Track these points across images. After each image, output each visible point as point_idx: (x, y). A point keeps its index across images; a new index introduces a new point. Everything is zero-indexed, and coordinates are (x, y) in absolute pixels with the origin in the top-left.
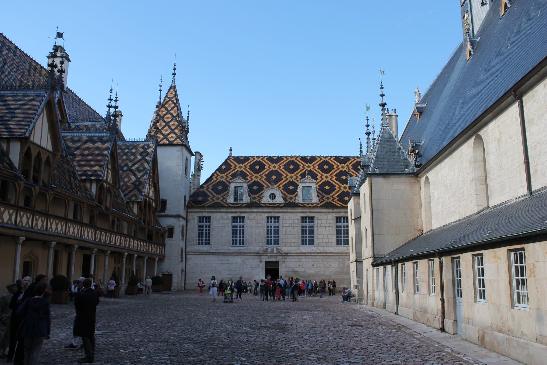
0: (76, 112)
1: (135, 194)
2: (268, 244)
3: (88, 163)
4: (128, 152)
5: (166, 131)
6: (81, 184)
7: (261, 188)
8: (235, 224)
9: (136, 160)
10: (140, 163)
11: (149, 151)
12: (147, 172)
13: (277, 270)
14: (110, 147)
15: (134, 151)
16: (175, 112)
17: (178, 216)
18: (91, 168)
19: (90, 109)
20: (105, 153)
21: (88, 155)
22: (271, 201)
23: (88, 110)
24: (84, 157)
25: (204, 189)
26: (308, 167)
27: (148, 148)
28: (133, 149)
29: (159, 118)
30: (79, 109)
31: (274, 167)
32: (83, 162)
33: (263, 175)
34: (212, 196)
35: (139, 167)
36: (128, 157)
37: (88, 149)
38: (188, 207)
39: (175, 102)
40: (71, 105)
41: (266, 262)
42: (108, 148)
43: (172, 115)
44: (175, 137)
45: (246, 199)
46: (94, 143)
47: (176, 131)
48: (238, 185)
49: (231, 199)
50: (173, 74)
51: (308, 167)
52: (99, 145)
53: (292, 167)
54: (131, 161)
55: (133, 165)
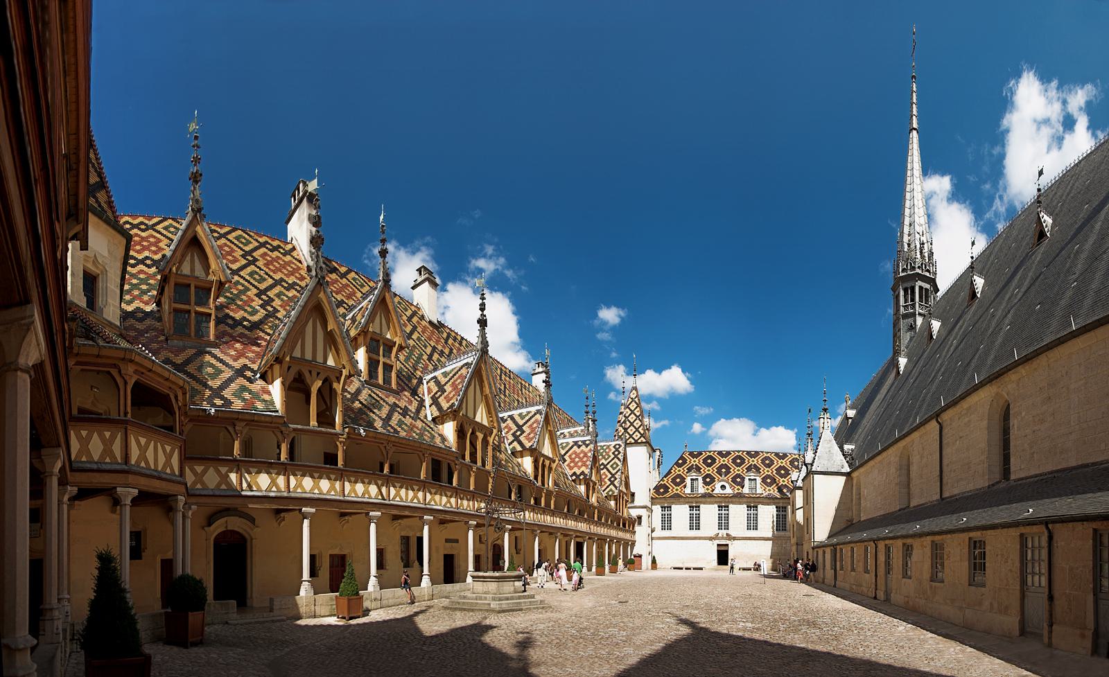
2: (719, 529)
3: (576, 465)
5: (631, 430)
7: (713, 480)
8: (692, 512)
9: (610, 459)
11: (620, 450)
13: (727, 552)
15: (607, 450)
17: (645, 507)
22: (722, 492)
24: (572, 461)
25: (665, 482)
26: (754, 461)
27: (619, 448)
31: (724, 461)
32: (572, 465)
33: (714, 469)
34: (671, 488)
35: (613, 465)
37: (575, 452)
38: (652, 498)
41: (718, 545)
44: (639, 435)
45: (702, 489)
46: (579, 447)
47: (640, 430)
48: (694, 477)
49: (688, 490)
51: (754, 461)
52: (583, 448)
53: (738, 461)
54: (606, 460)
55: (608, 463)
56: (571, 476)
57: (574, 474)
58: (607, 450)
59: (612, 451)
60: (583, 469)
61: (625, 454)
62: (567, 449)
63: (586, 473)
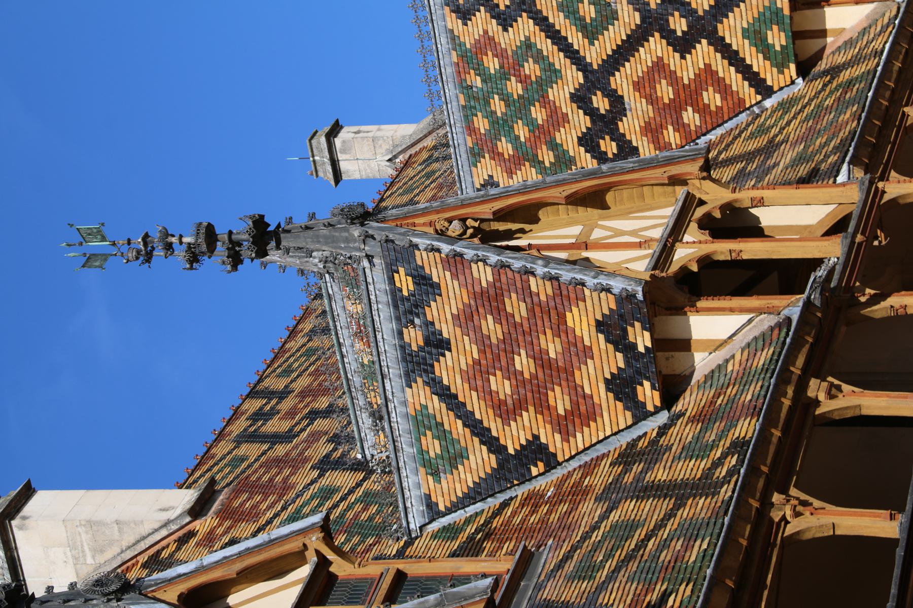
0: (314, 415)
1: (746, 33)
4: (506, 99)
6: (689, 402)
9: (545, 45)
14: (446, 248)
15: (492, 64)
18: (587, 352)
19: (307, 326)
20: (484, 275)
21: (511, 373)
23: (313, 332)
24: (531, 395)
28: (481, 71)
30: (303, 394)
32: (560, 401)
36: (538, 92)
37: (478, 374)
40: (281, 450)
42: (455, 262)
46: (438, 344)
52: (442, 313)
54: (552, 75)
56: (640, 413)
57: (621, 387)
58: (492, 64)
59: (494, 27)
60: (581, 321)
62: (458, 428)
63: (608, 303)
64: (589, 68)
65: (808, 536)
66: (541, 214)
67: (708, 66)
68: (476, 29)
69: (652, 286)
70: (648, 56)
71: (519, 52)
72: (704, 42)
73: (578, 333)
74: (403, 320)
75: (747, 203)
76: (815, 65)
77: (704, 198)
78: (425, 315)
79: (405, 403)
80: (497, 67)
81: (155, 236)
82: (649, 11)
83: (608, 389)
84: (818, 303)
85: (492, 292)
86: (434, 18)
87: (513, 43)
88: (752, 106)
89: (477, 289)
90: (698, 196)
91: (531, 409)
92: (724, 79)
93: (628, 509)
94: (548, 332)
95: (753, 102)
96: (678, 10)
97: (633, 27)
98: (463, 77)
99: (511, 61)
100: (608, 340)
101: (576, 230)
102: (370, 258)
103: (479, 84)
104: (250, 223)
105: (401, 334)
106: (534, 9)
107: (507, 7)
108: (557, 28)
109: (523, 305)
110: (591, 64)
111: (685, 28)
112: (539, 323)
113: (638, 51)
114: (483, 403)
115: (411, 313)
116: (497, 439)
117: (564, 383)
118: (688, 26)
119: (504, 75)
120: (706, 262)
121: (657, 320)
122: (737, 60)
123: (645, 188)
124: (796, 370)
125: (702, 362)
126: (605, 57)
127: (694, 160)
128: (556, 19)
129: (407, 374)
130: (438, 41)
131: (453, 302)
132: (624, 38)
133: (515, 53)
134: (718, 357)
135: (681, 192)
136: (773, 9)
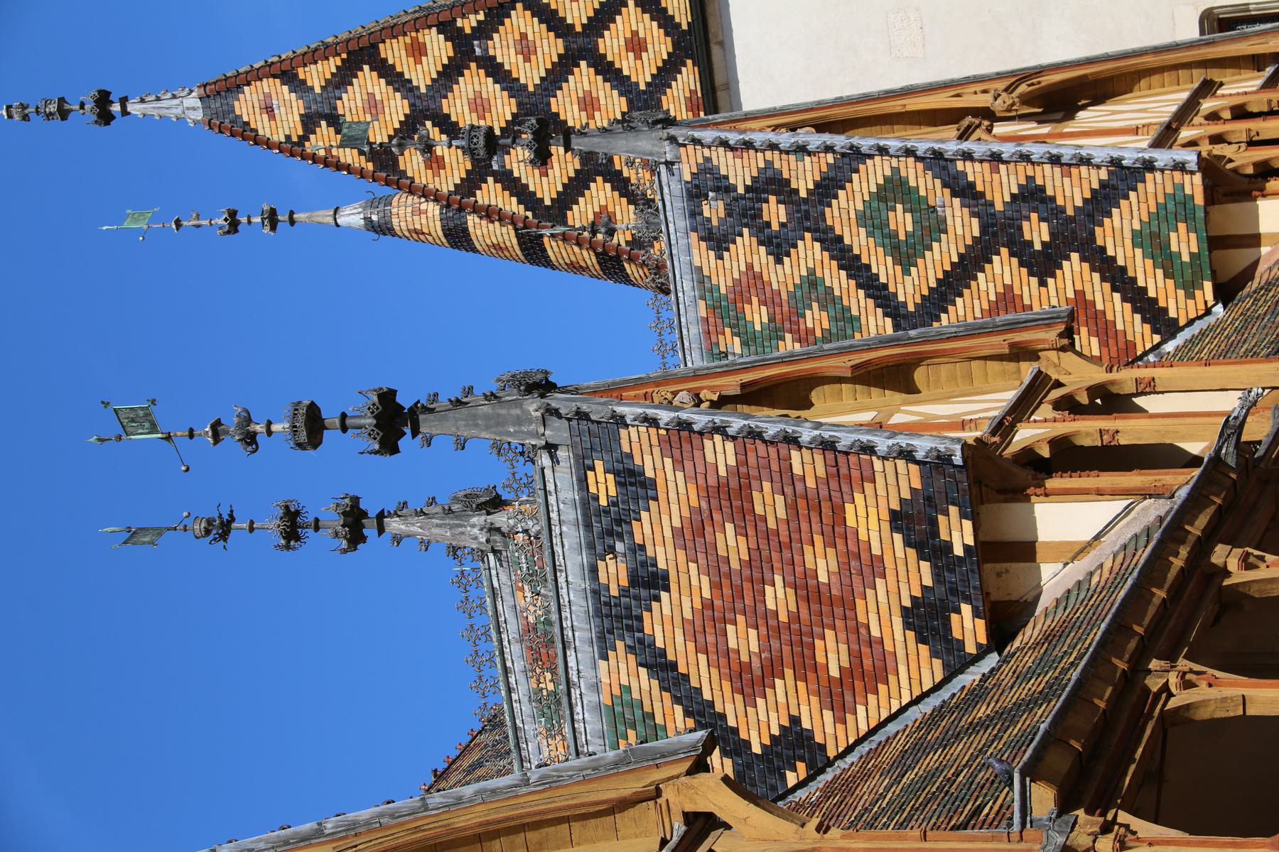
6: (1030, 633)
9: (837, 280)
10: (859, 241)
11: (739, 172)
12: (936, 161)
14: (665, 416)
15: (757, 316)
16: (417, 51)
18: (876, 567)
21: (760, 618)
24: (790, 651)
29: (491, 193)
32: (833, 654)
37: (707, 625)
39: (332, 64)
43: (450, 74)
46: (650, 581)
50: (105, 117)
52: (656, 530)
57: (927, 619)
58: (757, 316)
61: (790, 118)
63: (911, 478)
64: (902, 311)
65: (1203, 714)
66: (815, 396)
67: (1080, 294)
68: (735, 264)
69: (977, 452)
70: (991, 285)
71: (799, 294)
72: (1075, 256)
73: (863, 536)
74: (599, 548)
75: (1130, 388)
76: (1243, 288)
77: (1063, 379)
78: (632, 534)
79: (596, 687)
80: (765, 320)
81: (231, 422)
82: (993, 215)
83: (907, 626)
84: (1231, 461)
85: (734, 484)
86: (674, 252)
87: (790, 281)
88: (1146, 353)
89: (712, 481)
90: (1054, 377)
91: (789, 673)
92: (1104, 312)
93: (932, 760)
94: (818, 539)
95: (1148, 346)
96: (1035, 210)
97: (969, 242)
98: (714, 339)
99: (786, 308)
100: (908, 543)
101: (867, 417)
102: (551, 448)
103: (738, 350)
104: (375, 399)
105: (594, 570)
106: (822, 226)
107: (782, 225)
108: (856, 251)
109: (780, 499)
110: (905, 304)
111: (1046, 238)
112: (805, 526)
113: (976, 279)
114: (714, 671)
115: (610, 533)
116: (735, 731)
117: (839, 623)
118: (1051, 234)
119: (775, 332)
120: (1061, 445)
121: (983, 509)
122: (1124, 282)
123: (975, 364)
124: (1197, 528)
125: (1053, 578)
126: (926, 292)
127: (1048, 325)
128: (855, 239)
129: (602, 638)
130: (679, 288)
131: (674, 508)
132: (955, 259)
133: (792, 296)
134: (1077, 570)
135: (1028, 370)
136: (1179, 197)
